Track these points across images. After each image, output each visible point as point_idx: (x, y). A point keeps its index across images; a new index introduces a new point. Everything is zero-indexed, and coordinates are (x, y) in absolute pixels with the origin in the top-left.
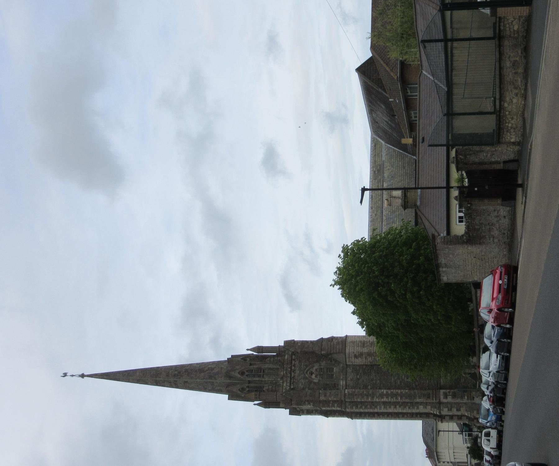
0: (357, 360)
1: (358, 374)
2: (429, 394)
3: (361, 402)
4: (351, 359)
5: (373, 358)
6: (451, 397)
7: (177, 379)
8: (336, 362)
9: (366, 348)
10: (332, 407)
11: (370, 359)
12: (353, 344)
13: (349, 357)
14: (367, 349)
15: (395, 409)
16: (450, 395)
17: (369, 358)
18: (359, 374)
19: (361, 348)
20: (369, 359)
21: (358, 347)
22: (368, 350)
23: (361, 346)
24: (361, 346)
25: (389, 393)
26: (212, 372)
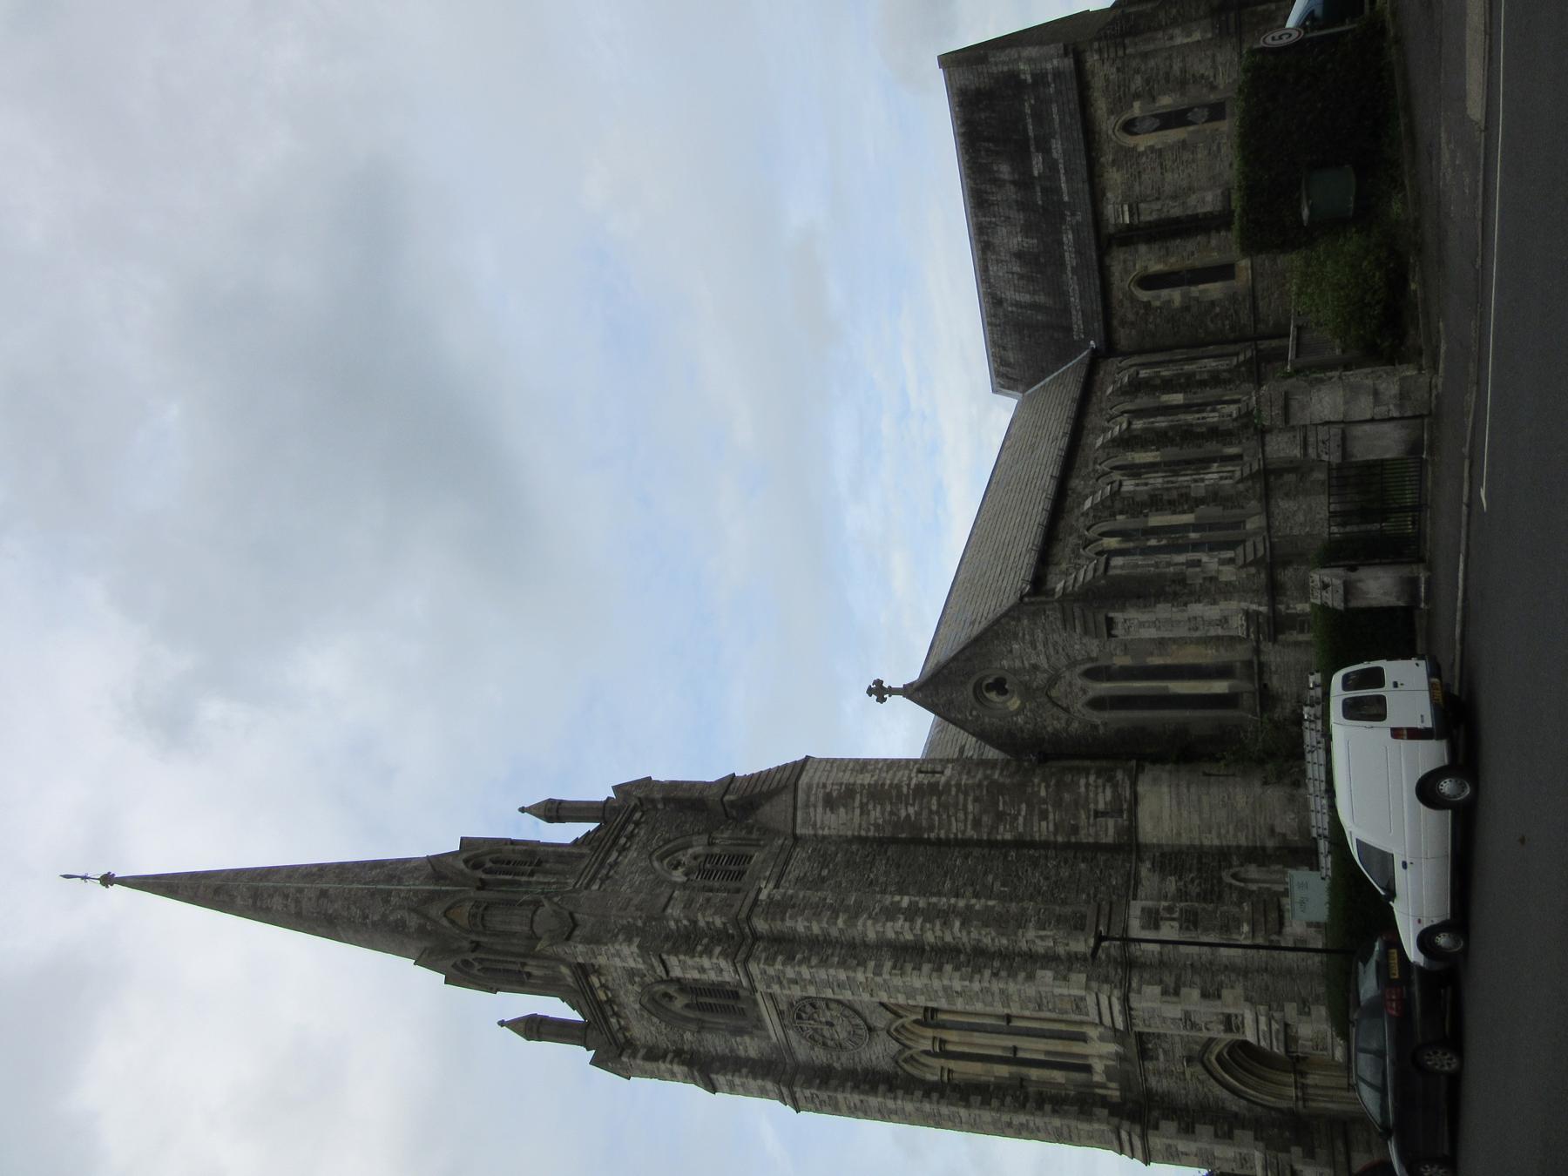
0: (833, 817)
1: (828, 866)
2: (1084, 917)
5: (888, 808)
6: (1176, 924)
9: (867, 775)
13: (807, 806)
14: (872, 776)
17: (875, 807)
18: (831, 866)
20: (873, 813)
21: (844, 771)
22: (876, 778)
23: (852, 770)
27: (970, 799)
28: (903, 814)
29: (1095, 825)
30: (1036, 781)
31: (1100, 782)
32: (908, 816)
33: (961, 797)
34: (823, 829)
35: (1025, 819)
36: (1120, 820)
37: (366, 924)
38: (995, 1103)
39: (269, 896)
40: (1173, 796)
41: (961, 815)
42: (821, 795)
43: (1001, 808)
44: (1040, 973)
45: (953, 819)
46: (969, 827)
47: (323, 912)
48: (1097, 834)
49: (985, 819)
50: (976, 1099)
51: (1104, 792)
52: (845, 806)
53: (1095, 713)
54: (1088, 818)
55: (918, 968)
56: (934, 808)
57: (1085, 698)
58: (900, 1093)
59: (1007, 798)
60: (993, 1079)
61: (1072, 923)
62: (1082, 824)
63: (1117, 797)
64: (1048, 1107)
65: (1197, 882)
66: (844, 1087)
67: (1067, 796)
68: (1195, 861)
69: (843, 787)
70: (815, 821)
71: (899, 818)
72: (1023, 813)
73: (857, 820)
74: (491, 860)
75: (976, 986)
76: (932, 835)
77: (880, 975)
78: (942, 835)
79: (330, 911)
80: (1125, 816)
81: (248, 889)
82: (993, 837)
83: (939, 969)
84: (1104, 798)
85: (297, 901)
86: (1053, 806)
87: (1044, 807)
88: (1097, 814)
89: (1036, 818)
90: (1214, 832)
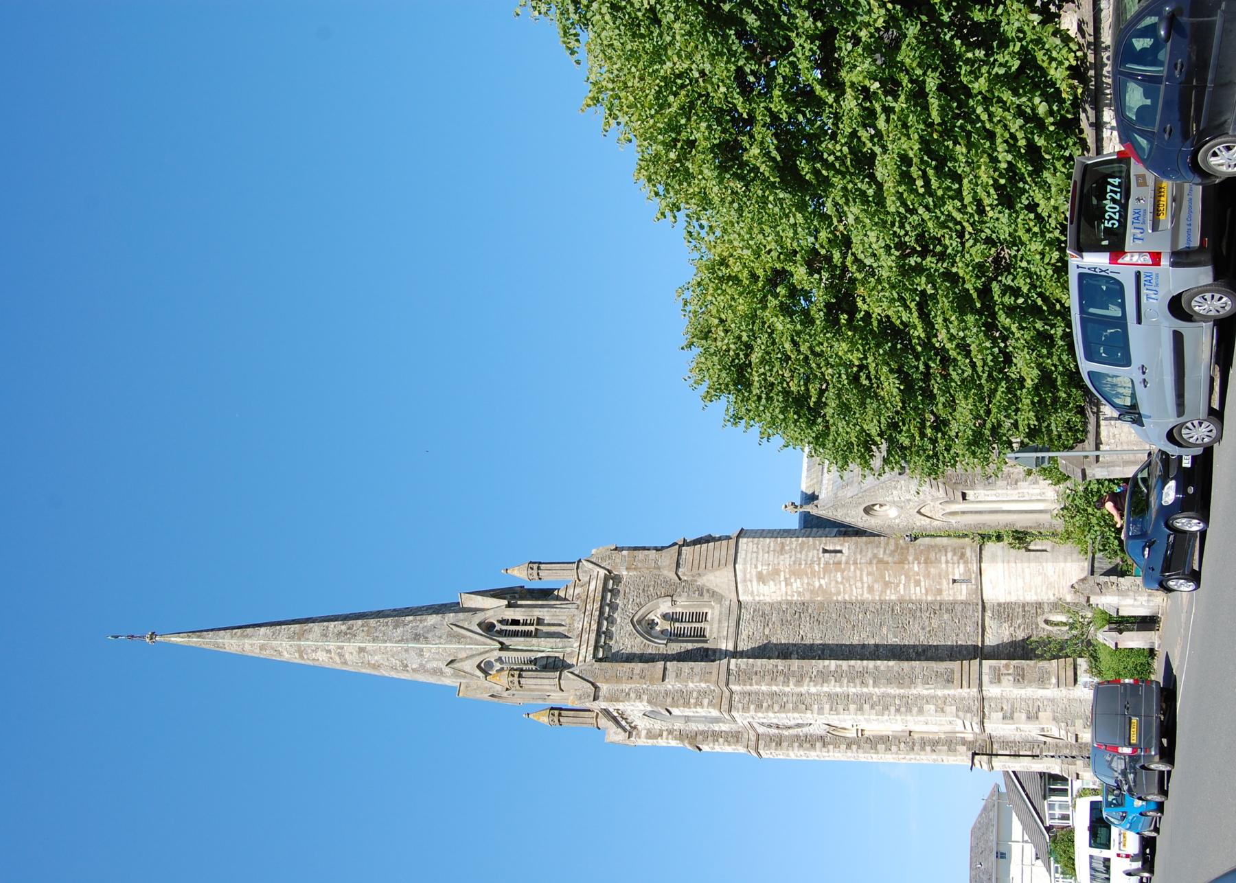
0: (766, 587)
4: (749, 584)
5: (806, 581)
7: (342, 642)
8: (713, 596)
9: (787, 556)
11: (799, 586)
12: (755, 546)
13: (744, 581)
14: (791, 557)
18: (770, 625)
19: (774, 555)
20: (794, 585)
21: (768, 552)
22: (793, 559)
23: (774, 551)
24: (774, 551)
26: (421, 626)
28: (817, 584)
30: (911, 558)
31: (955, 558)
32: (821, 585)
33: (858, 573)
35: (904, 585)
36: (970, 586)
37: (407, 671)
38: (894, 748)
40: (1006, 568)
41: (859, 584)
42: (754, 573)
43: (887, 579)
45: (854, 587)
49: (876, 586)
50: (881, 747)
51: (958, 567)
54: (948, 584)
56: (839, 580)
57: (944, 512)
58: (831, 747)
59: (891, 572)
60: (891, 733)
62: (944, 588)
63: (968, 571)
64: (928, 748)
67: (933, 571)
68: (1020, 610)
69: (770, 567)
70: (752, 592)
71: (814, 587)
72: (903, 582)
76: (840, 598)
77: (823, 714)
78: (847, 598)
79: (373, 662)
80: (973, 582)
81: (291, 646)
82: (882, 598)
84: (958, 571)
86: (924, 577)
87: (918, 577)
88: (954, 581)
89: (912, 585)
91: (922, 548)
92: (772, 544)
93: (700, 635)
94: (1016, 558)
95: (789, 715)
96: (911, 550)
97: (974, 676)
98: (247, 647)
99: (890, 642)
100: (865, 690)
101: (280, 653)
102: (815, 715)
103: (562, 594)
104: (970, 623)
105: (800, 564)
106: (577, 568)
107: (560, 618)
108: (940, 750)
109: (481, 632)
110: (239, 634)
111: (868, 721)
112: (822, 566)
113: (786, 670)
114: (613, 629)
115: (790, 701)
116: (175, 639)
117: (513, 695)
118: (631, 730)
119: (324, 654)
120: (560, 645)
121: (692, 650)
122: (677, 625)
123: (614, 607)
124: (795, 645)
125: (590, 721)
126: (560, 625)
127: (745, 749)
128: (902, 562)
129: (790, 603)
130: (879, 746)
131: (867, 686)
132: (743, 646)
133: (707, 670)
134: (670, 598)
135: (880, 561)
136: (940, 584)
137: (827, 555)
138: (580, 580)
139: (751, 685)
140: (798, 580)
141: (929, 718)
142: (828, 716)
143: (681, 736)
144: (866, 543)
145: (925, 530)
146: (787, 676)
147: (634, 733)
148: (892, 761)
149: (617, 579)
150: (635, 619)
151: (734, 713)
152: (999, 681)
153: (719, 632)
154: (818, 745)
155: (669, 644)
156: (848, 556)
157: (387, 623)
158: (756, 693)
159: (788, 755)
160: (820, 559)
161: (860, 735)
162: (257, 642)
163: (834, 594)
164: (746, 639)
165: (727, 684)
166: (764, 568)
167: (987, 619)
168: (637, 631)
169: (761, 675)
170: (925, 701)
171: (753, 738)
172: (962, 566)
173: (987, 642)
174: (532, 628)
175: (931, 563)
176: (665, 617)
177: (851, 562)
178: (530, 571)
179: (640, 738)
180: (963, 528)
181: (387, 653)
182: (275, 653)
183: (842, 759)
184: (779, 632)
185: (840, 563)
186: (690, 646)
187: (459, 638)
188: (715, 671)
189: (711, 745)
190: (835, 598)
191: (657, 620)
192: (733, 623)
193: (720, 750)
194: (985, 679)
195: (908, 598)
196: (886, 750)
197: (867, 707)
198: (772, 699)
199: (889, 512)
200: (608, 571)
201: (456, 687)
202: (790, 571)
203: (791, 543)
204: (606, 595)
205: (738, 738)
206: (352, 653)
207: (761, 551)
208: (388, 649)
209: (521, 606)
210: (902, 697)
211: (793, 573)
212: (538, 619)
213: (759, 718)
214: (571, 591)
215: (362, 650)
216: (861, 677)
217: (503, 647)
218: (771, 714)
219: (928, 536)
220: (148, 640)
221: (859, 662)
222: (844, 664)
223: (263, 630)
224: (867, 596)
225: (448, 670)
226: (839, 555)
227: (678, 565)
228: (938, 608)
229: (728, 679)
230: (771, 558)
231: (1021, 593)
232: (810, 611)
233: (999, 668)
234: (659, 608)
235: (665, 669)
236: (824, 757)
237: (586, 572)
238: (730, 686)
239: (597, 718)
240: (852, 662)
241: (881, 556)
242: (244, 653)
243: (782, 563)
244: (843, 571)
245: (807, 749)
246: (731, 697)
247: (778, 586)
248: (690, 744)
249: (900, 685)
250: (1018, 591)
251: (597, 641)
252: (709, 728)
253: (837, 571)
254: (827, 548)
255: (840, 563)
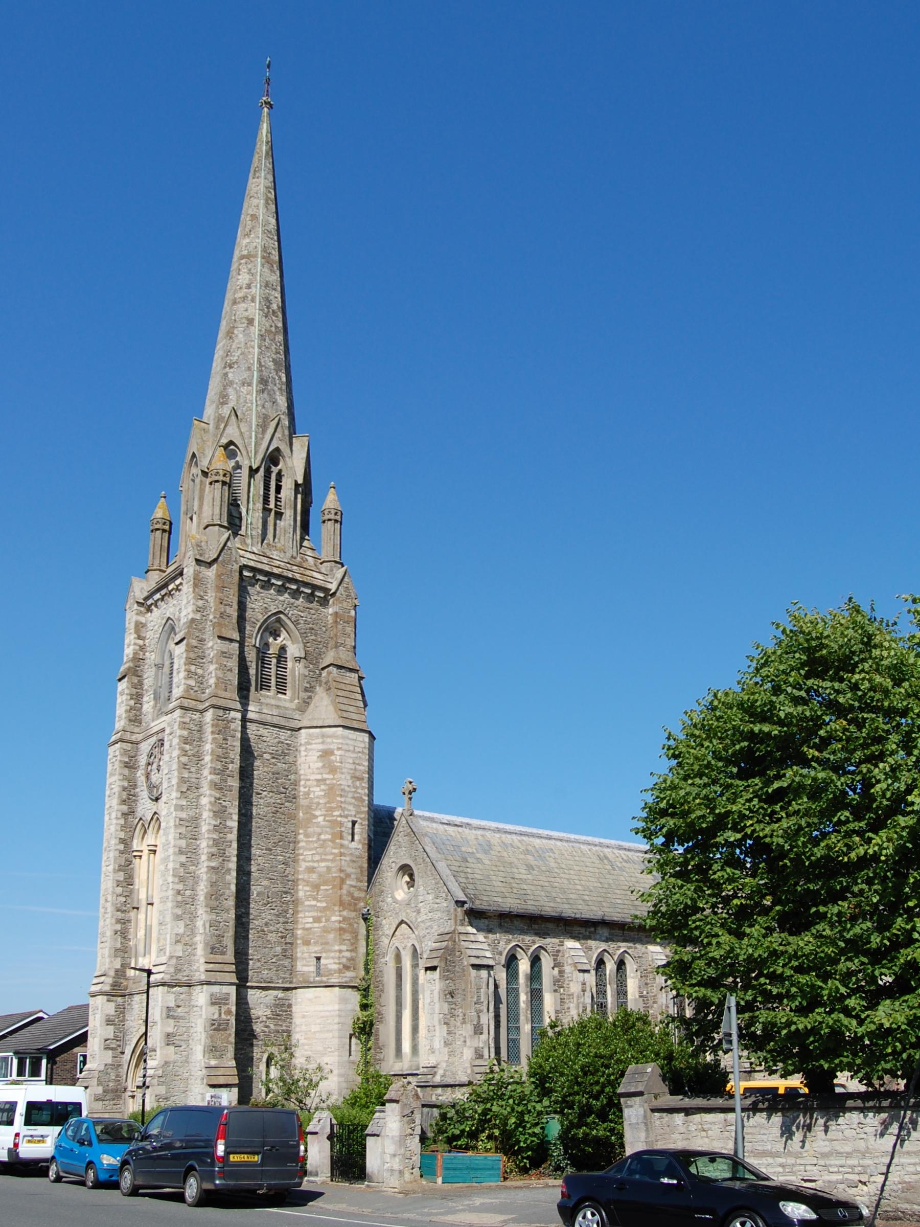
1: (273, 758)
2: (223, 953)
3: (199, 757)
5: (321, 801)
8: (304, 702)
9: (350, 783)
10: (189, 671)
11: (316, 794)
12: (360, 750)
13: (323, 736)
14: (349, 786)
15: (177, 850)
16: (220, 1014)
17: (323, 790)
18: (273, 760)
20: (318, 789)
21: (354, 763)
22: (347, 789)
23: (355, 769)
24: (355, 769)
25: (229, 835)
27: (329, 864)
28: (317, 813)
29: (310, 957)
30: (345, 913)
31: (344, 960)
32: (317, 817)
33: (330, 857)
34: (306, 750)
35: (315, 906)
37: (225, 367)
38: (119, 890)
39: (250, 270)
41: (317, 858)
42: (332, 747)
43: (322, 887)
44: (181, 924)
46: (308, 864)
47: (235, 325)
48: (303, 959)
50: (121, 876)
52: (324, 766)
53: (393, 956)
54: (315, 952)
55: (181, 836)
56: (322, 837)
57: (400, 949)
58: (122, 822)
60: (137, 887)
61: (217, 946)
62: (311, 947)
63: (330, 973)
64: (118, 927)
65: (266, 1029)
66: (123, 780)
67: (331, 936)
68: (284, 1028)
70: (311, 744)
71: (315, 810)
72: (319, 904)
73: (312, 777)
74: (280, 471)
75: (170, 879)
76: (301, 837)
78: (301, 844)
79: (236, 332)
80: (317, 979)
82: (300, 882)
83: (181, 852)
85: (244, 298)
86: (324, 926)
87: (324, 920)
88: (318, 959)
89: (315, 914)
90: (306, 1041)
91: (355, 925)
92: (361, 768)
93: (263, 685)
94: (343, 1024)
95: (176, 773)
96: (353, 914)
97: (220, 977)
98: (255, 202)
99: (253, 888)
100: (204, 858)
101: (247, 235)
102: (174, 802)
103: (305, 543)
104: (272, 974)
105: (341, 796)
106: (336, 562)
107: (282, 538)
108: (116, 939)
109: (271, 449)
110: (269, 195)
111: (165, 860)
112: (339, 819)
113: (228, 772)
114: (272, 591)
115: (190, 775)
116: (265, 128)
117: (193, 481)
118: (146, 605)
119: (247, 281)
120: (254, 533)
121: (248, 673)
122: (274, 661)
123: (296, 594)
124: (251, 784)
125: (157, 562)
126: (275, 536)
127: (121, 728)
128: (341, 903)
129: (296, 783)
130: (122, 874)
131: (209, 859)
132: (252, 728)
133: (229, 687)
134: (303, 656)
135: (343, 881)
136: (316, 943)
137: (350, 825)
138: (321, 563)
139: (213, 733)
140: (323, 793)
141: (169, 926)
142: (174, 815)
143: (138, 660)
144: (361, 867)
145: (376, 929)
146: (221, 773)
147: (142, 609)
148: (103, 887)
149: (324, 602)
150: (282, 616)
151: (178, 712)
152: (213, 1004)
153: (267, 705)
154: (125, 808)
155: (255, 649)
156: (348, 848)
157: (279, 353)
158: (200, 739)
159: (112, 775)
160: (346, 817)
161: (135, 854)
162: (261, 212)
163: (306, 831)
164: (259, 733)
165: (213, 706)
166: (338, 758)
167: (275, 993)
168: (269, 617)
169: (222, 745)
170: (189, 923)
171: (134, 738)
172: (336, 967)
173: (251, 992)
174: (272, 505)
175: (340, 935)
176: (283, 649)
177: (342, 850)
178: (333, 512)
179: (137, 614)
180: (378, 970)
181: (247, 348)
182: (247, 230)
183: (105, 834)
184: (266, 769)
185: (341, 838)
186: (252, 672)
187: (263, 427)
188: (228, 695)
189: (127, 691)
190: (301, 831)
191: (280, 640)
192: (276, 720)
193: (119, 701)
194: (216, 989)
195: (300, 909)
196: (118, 881)
197: (183, 859)
198: (194, 756)
199: (400, 891)
200: (334, 593)
201: (202, 417)
202: (334, 785)
203: (363, 788)
204: (308, 588)
205: (134, 721)
206: (246, 310)
207: (355, 755)
208: (251, 350)
209: (296, 498)
210: (193, 898)
211: (331, 788)
212: (282, 514)
213: (171, 740)
214: (309, 553)
215: (251, 322)
216: (219, 853)
217: (253, 472)
218: (176, 753)
219: (368, 931)
220: (264, 98)
221: (235, 852)
222: (233, 836)
223: (274, 221)
224: (303, 866)
225: (226, 411)
226: (350, 838)
227: (340, 667)
228: (288, 940)
229: (219, 708)
230: (348, 766)
231: (304, 1028)
232: (287, 804)
233: (227, 1004)
234: (293, 643)
235: (231, 640)
236: (110, 814)
237: (332, 570)
238: (211, 710)
239: (161, 570)
240: (235, 845)
241: (348, 882)
242: (246, 199)
243: (343, 776)
244: (332, 841)
245: (120, 796)
246: (197, 711)
247: (316, 771)
248: (129, 669)
249: (210, 896)
250: (306, 1025)
251: (261, 571)
252: (147, 691)
253: (333, 834)
254: (357, 826)
255: (341, 838)
